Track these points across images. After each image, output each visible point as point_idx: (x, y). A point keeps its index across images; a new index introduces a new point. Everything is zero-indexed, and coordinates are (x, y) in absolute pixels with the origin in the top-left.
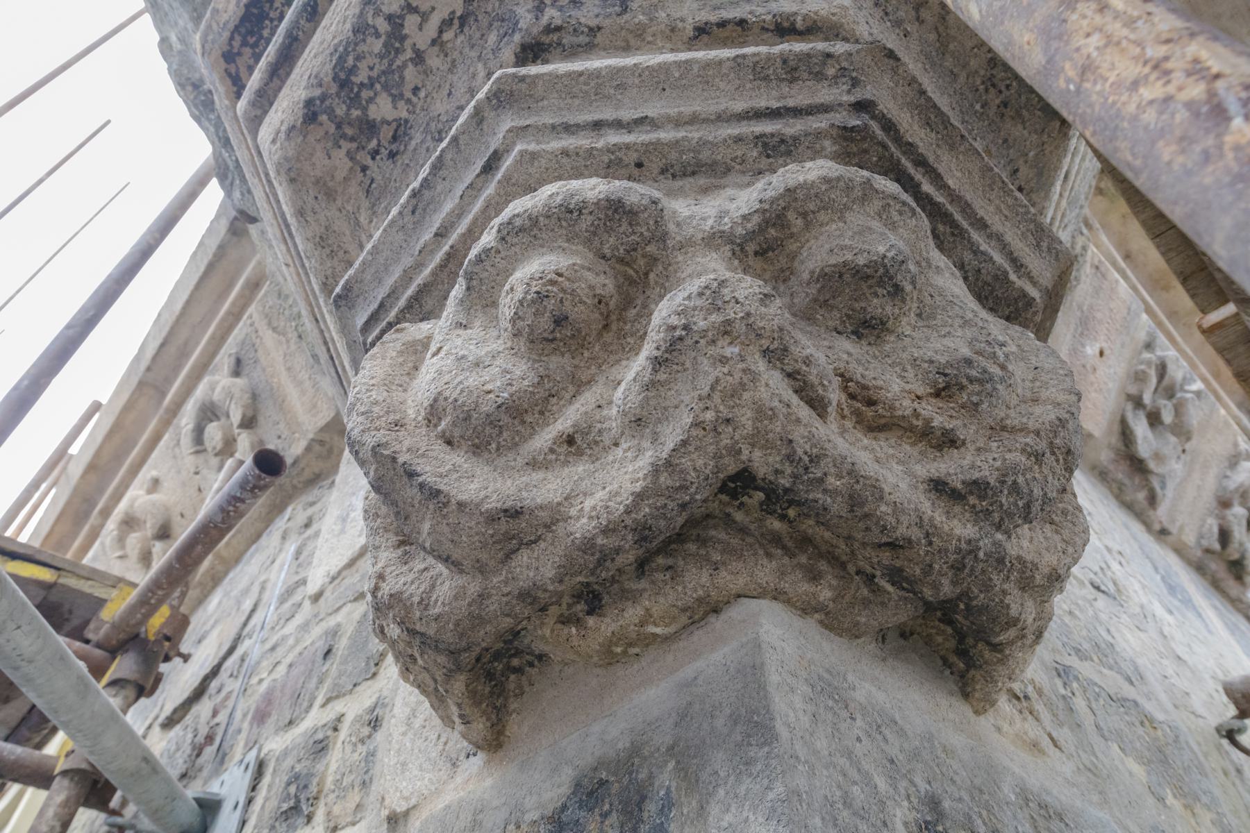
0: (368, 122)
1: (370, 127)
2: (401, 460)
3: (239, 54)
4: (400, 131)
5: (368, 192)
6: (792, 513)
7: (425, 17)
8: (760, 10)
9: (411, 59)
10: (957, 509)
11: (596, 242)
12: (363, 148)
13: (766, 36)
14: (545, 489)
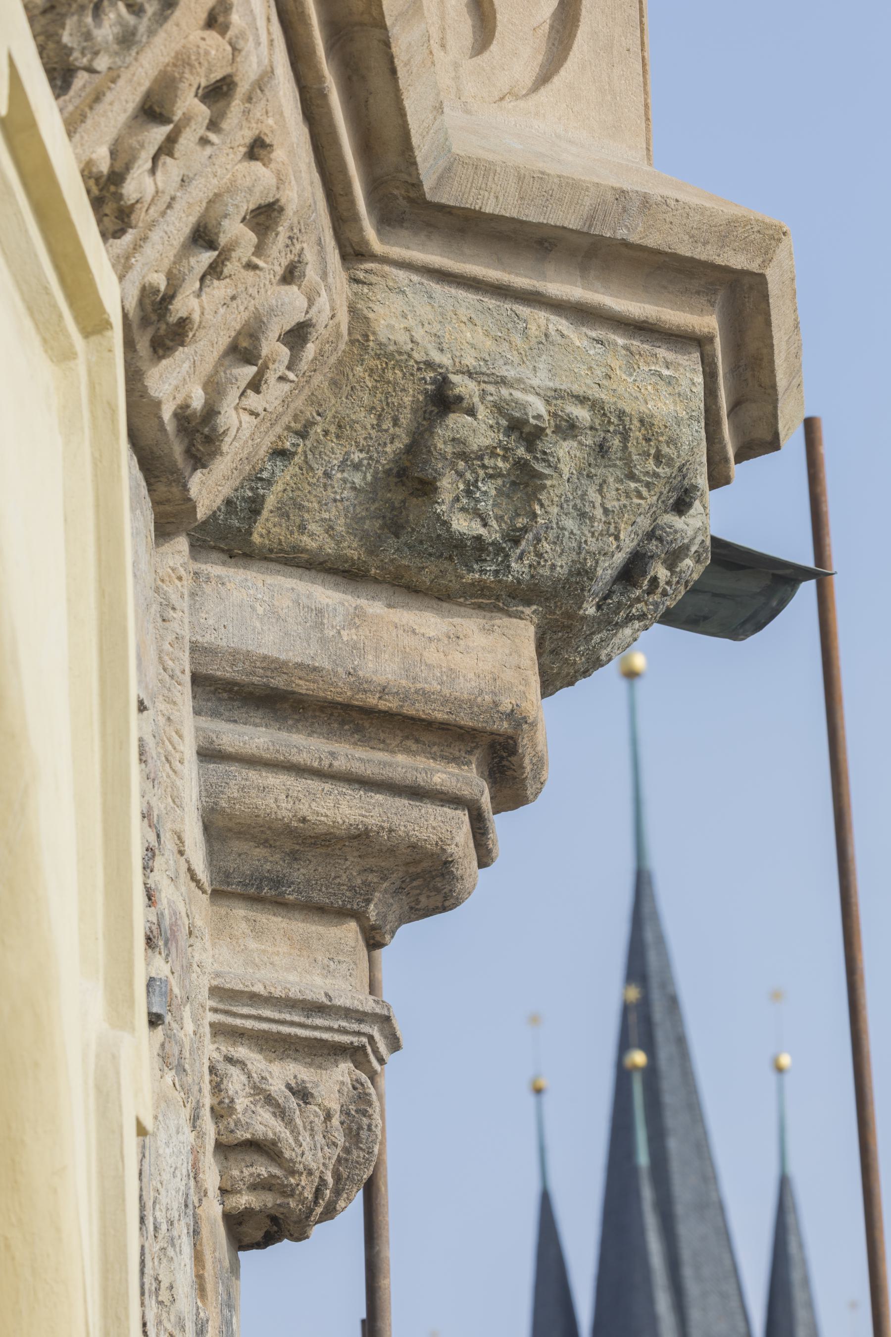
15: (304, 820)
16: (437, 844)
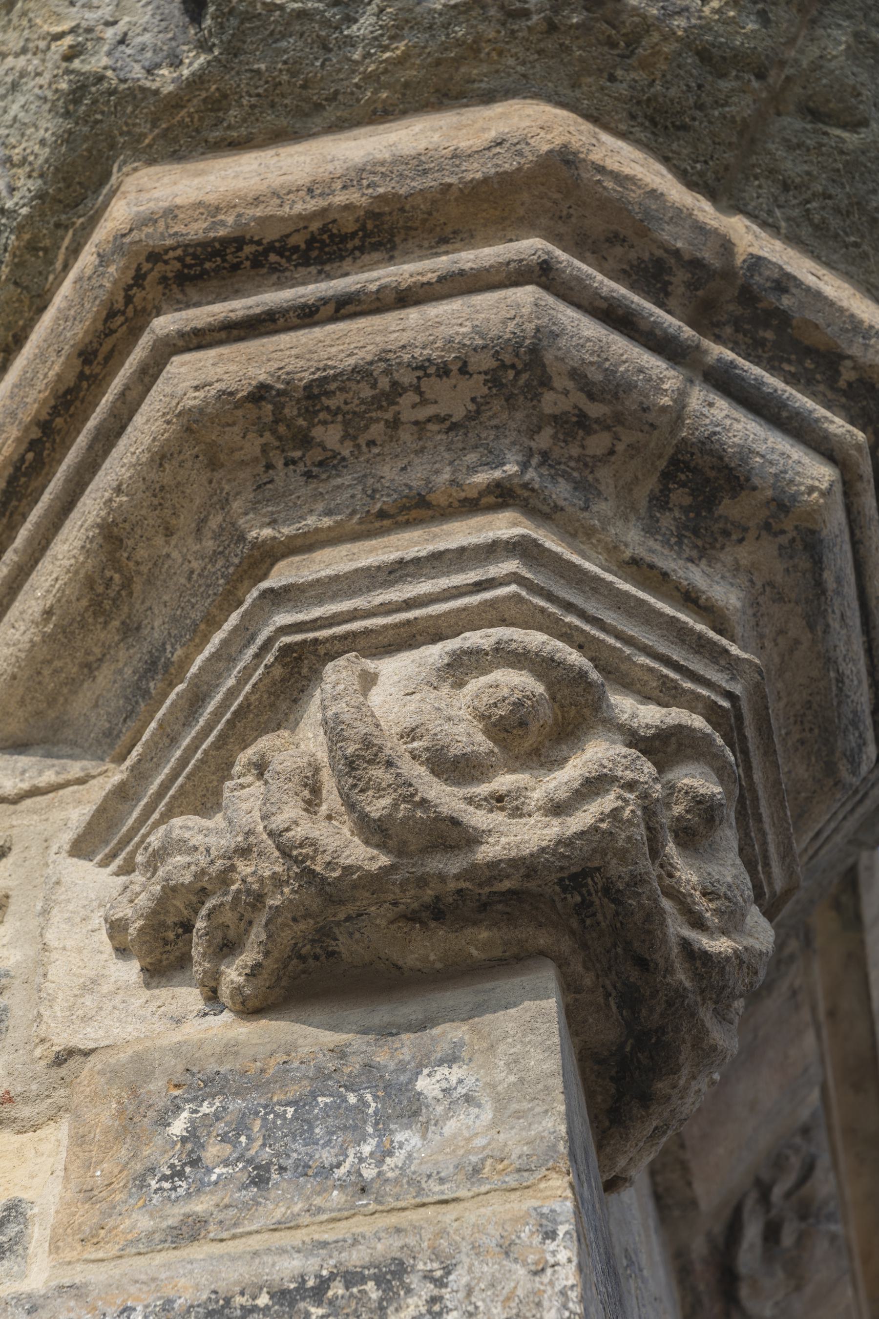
0: (306, 436)
1: (305, 441)
2: (387, 752)
3: (166, 262)
4: (331, 463)
5: (259, 487)
6: (588, 922)
7: (424, 402)
8: (681, 573)
9: (387, 421)
10: (687, 965)
11: (556, 688)
12: (283, 451)
13: (676, 593)
14: (479, 819)
15: (48, 613)
16: (168, 422)
